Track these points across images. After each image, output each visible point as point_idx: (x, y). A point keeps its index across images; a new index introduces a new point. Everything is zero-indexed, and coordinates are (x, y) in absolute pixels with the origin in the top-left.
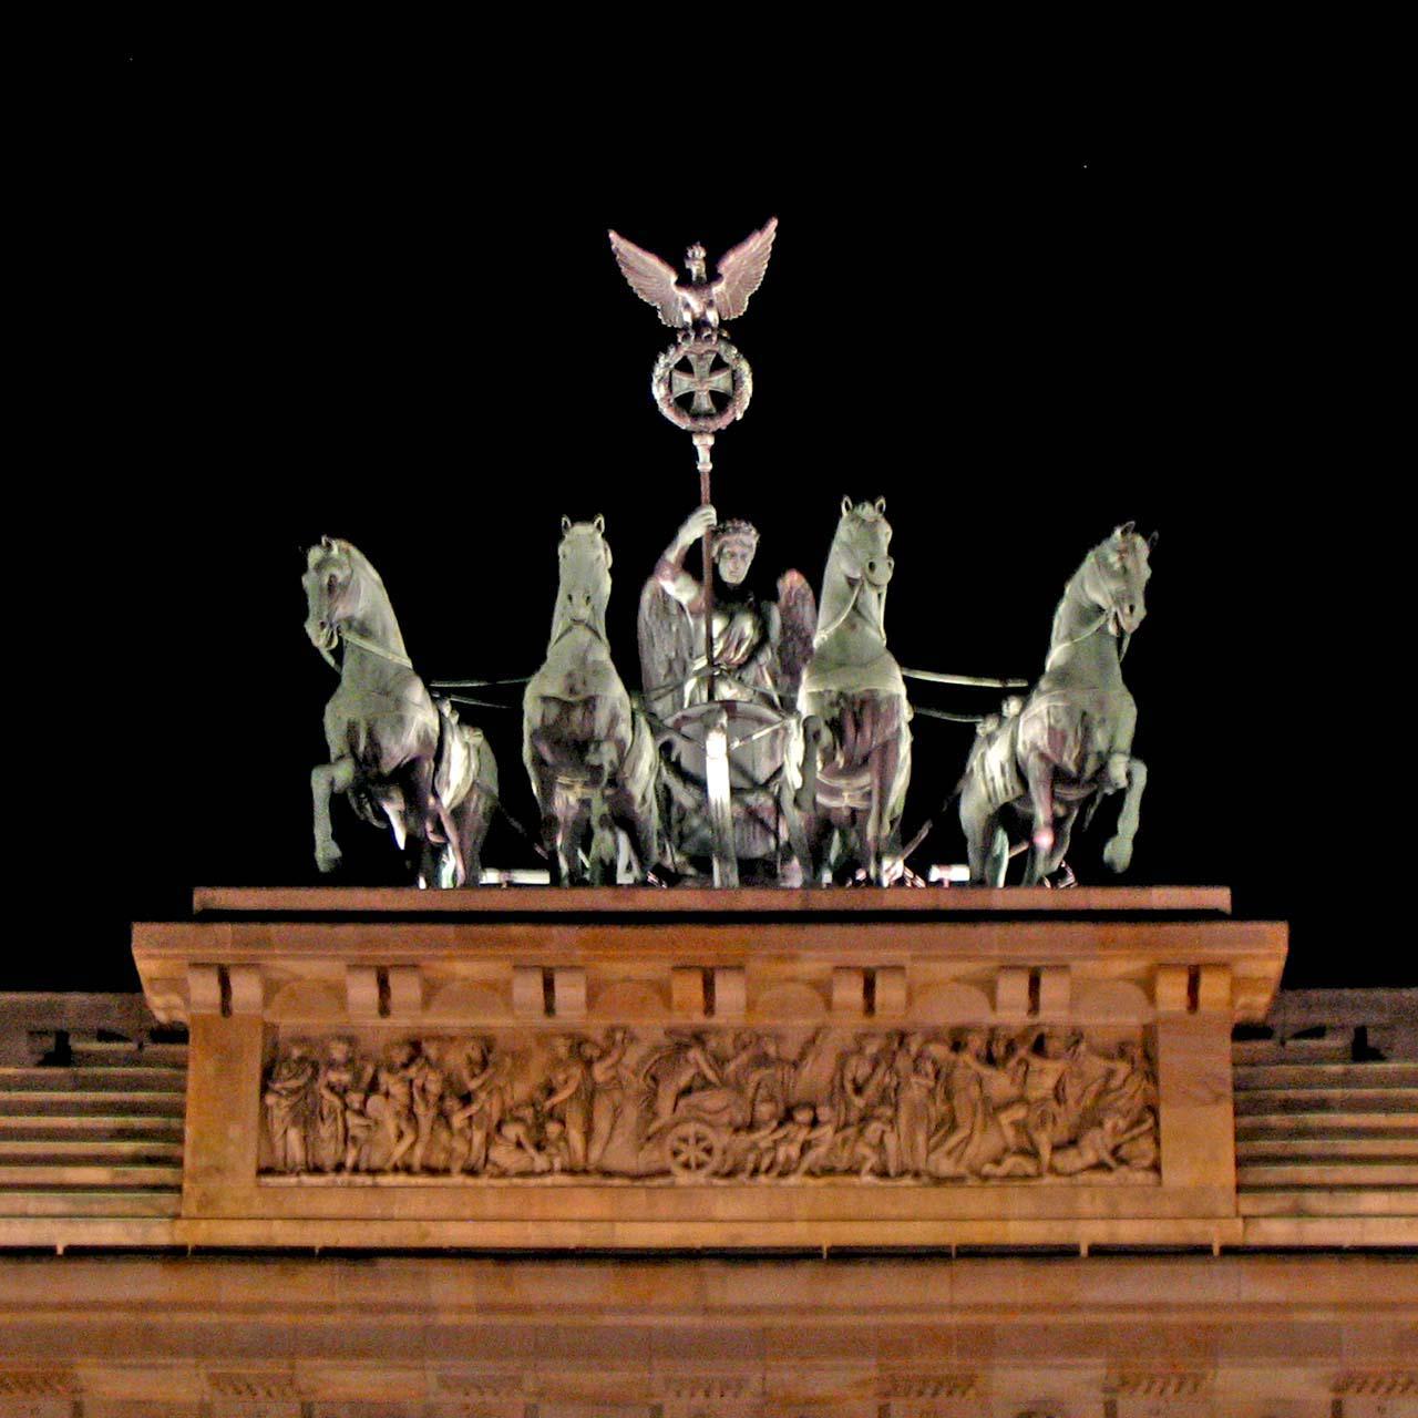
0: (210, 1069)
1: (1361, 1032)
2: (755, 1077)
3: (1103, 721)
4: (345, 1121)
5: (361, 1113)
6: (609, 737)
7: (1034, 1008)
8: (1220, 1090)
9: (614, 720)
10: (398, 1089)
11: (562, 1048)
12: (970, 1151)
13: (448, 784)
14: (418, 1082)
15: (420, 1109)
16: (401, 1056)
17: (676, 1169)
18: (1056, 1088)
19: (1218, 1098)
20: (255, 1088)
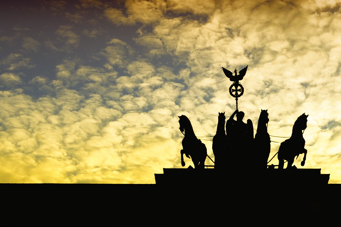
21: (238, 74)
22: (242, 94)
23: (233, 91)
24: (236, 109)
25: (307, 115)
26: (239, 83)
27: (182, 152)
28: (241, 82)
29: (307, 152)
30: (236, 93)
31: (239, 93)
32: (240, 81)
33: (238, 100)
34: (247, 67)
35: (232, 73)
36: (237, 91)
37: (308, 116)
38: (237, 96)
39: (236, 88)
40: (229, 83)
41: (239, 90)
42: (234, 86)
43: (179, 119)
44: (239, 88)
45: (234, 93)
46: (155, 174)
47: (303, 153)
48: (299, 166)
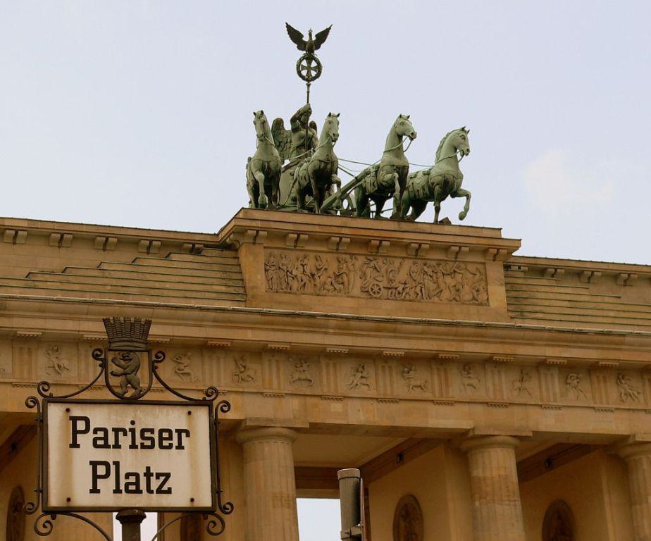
0: (251, 259)
7: (456, 258)
10: (301, 269)
14: (305, 267)
17: (373, 294)
21: (314, 38)
22: (317, 76)
23: (304, 68)
31: (314, 73)
32: (316, 52)
33: (311, 86)
34: (330, 28)
35: (302, 36)
36: (310, 70)
38: (309, 79)
39: (309, 63)
41: (314, 69)
42: (305, 60)
44: (314, 64)
45: (304, 73)
47: (460, 196)
48: (455, 221)
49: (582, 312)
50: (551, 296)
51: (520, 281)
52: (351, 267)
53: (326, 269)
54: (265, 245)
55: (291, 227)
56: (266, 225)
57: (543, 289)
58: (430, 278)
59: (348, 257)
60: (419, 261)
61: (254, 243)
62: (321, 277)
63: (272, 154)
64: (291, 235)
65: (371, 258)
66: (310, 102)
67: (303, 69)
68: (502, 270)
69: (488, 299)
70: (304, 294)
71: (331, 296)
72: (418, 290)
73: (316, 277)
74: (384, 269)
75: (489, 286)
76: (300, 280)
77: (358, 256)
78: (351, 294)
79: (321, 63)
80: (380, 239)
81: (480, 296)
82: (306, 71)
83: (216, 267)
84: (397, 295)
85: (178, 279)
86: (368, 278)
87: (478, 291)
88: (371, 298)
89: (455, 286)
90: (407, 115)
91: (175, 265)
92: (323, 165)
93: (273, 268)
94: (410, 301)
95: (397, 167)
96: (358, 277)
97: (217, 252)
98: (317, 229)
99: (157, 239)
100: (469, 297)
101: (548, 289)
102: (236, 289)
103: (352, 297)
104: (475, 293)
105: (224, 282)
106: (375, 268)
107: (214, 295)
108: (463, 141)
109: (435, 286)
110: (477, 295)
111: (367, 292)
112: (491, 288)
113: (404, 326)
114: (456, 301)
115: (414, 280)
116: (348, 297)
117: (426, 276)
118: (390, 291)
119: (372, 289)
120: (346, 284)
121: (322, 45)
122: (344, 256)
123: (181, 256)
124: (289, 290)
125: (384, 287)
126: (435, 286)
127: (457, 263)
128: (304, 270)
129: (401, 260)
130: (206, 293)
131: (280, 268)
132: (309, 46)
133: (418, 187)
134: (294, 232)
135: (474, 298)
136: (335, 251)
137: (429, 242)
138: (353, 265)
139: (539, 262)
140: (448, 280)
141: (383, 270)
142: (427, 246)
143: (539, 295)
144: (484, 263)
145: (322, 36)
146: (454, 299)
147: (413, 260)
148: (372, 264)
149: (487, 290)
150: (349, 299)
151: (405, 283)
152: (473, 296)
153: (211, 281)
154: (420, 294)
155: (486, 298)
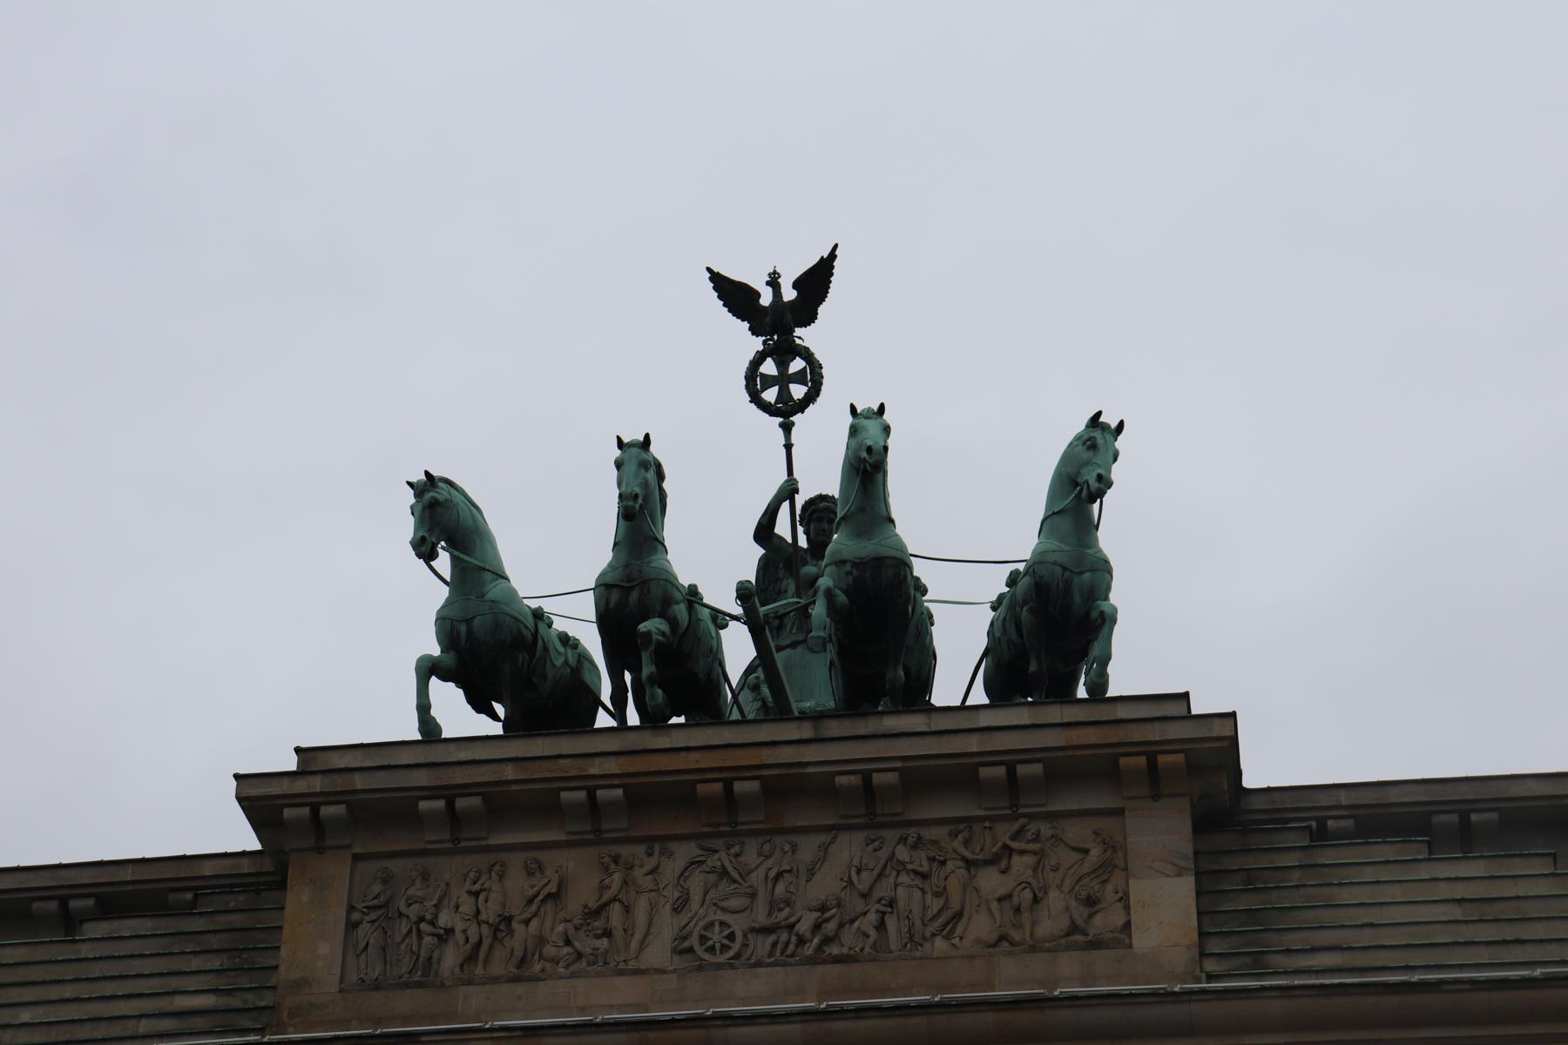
1: (1322, 822)
2: (772, 874)
3: (1082, 573)
4: (419, 932)
5: (432, 923)
6: (662, 615)
8: (1182, 863)
9: (668, 601)
10: (467, 907)
11: (607, 859)
12: (959, 929)
13: (545, 677)
14: (482, 897)
15: (483, 917)
16: (472, 875)
17: (706, 956)
18: (1035, 870)
19: (1180, 875)
20: (342, 911)
21: (789, 294)
23: (768, 382)
24: (785, 477)
25: (1114, 425)
26: (798, 341)
27: (428, 670)
28: (805, 336)
29: (1114, 621)
30: (784, 395)
31: (798, 391)
32: (798, 331)
33: (794, 430)
34: (832, 256)
35: (758, 295)
37: (1121, 426)
38: (786, 411)
39: (782, 365)
40: (744, 342)
41: (799, 378)
43: (409, 497)
44: (797, 365)
45: (770, 395)
46: (237, 776)
49: (1509, 932)
50: (1395, 893)
51: (1290, 860)
52: (647, 882)
53: (554, 897)
54: (356, 850)
55: (422, 779)
56: (340, 783)
57: (1369, 874)
58: (918, 881)
59: (640, 850)
60: (890, 835)
61: (320, 850)
62: (534, 923)
63: (483, 596)
64: (424, 805)
65: (717, 843)
66: (796, 475)
67: (764, 389)
68: (1186, 826)
69: (1128, 925)
70: (470, 983)
71: (561, 978)
72: (873, 917)
73: (515, 925)
74: (761, 872)
75: (1131, 882)
76: (460, 937)
77: (673, 846)
78: (632, 964)
79: (819, 356)
80: (724, 775)
81: (1098, 920)
82: (775, 389)
83: (214, 942)
84: (791, 947)
85: (68, 991)
86: (695, 905)
87: (1091, 902)
88: (700, 968)
89: (1010, 896)
90: (875, 408)
91: (85, 950)
92: (615, 596)
93: (373, 916)
94: (837, 960)
95: (854, 564)
96: (668, 907)
97: (241, 898)
98: (509, 772)
99: (80, 890)
100: (1050, 923)
101: (1385, 874)
102: (250, 997)
103: (636, 972)
104: (1079, 913)
105: (220, 982)
106: (724, 873)
107: (167, 1025)
108: (1089, 454)
109: (936, 904)
110: (1091, 916)
111: (691, 950)
112: (1137, 890)
113: (734, 1032)
114: (1012, 944)
115: (864, 896)
116: (620, 973)
117: (904, 878)
118: (772, 938)
119: (703, 939)
120: (618, 934)
121: (820, 310)
122: (626, 851)
123: (115, 924)
124: (425, 975)
125: (753, 930)
126: (936, 904)
127: (1022, 821)
128: (478, 912)
129: (822, 838)
130: (143, 1022)
131: (401, 914)
132: (779, 320)
133: (997, 635)
134: (432, 792)
135: (1074, 929)
136: (591, 836)
137: (898, 764)
138: (653, 871)
139: (1393, 796)
140: (991, 882)
141: (756, 878)
142: (892, 777)
143: (1346, 896)
144: (1120, 812)
145: (816, 282)
146: (1003, 938)
147: (866, 833)
148: (713, 861)
149: (1127, 895)
150: (619, 981)
151: (823, 908)
152: (1073, 921)
153: (175, 983)
154: (872, 933)
155: (1121, 922)
